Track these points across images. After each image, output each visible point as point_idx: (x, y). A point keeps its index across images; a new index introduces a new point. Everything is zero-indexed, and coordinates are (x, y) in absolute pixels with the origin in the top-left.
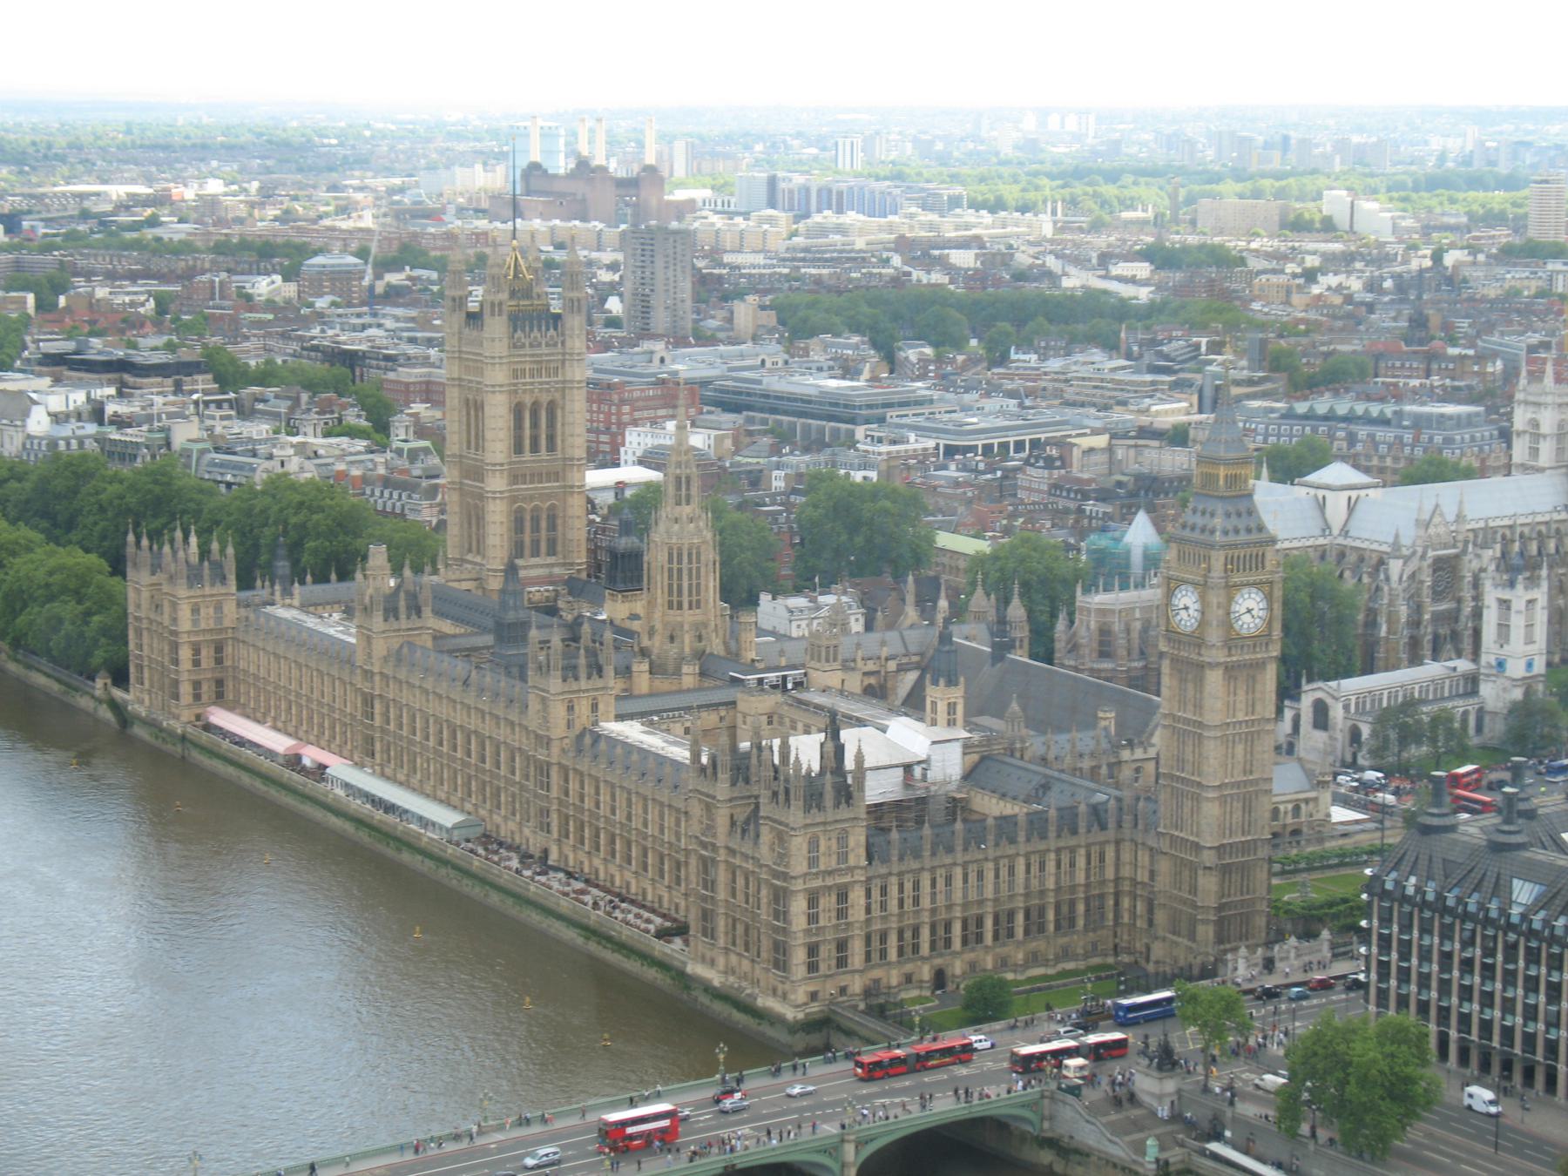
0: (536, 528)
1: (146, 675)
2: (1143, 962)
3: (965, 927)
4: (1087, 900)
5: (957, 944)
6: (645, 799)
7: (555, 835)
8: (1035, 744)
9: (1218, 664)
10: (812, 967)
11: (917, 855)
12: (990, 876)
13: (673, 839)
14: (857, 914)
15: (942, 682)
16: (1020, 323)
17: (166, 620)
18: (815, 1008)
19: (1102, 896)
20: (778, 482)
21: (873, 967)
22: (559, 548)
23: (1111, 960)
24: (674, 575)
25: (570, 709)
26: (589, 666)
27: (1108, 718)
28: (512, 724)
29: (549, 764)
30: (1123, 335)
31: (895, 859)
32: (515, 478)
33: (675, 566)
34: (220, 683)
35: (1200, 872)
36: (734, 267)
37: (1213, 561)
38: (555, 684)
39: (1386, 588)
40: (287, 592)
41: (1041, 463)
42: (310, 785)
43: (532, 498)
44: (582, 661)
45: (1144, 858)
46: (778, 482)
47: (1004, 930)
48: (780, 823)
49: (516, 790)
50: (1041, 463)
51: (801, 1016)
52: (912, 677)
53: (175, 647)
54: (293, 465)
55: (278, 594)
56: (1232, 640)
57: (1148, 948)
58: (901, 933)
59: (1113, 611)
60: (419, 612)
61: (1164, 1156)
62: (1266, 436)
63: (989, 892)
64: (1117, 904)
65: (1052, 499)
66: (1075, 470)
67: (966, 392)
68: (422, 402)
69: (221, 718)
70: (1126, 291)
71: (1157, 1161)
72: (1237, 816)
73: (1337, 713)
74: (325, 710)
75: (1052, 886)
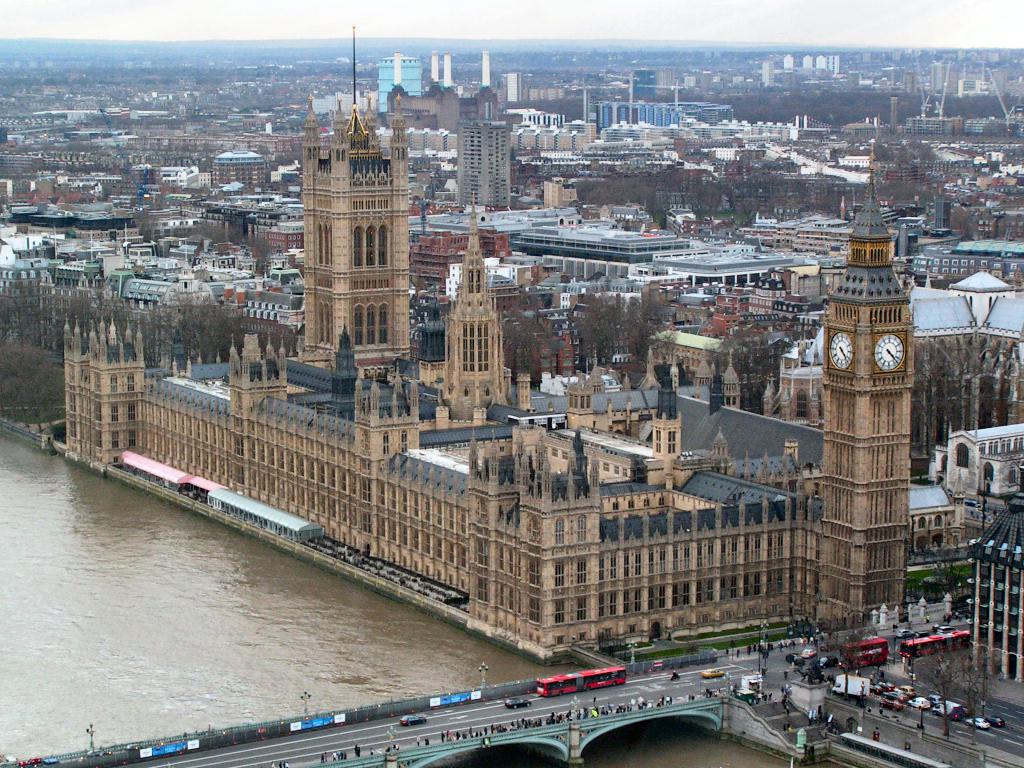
0: (371, 322)
2: (811, 620)
3: (675, 591)
5: (669, 604)
6: (440, 503)
7: (375, 534)
9: (865, 392)
10: (559, 618)
12: (694, 552)
13: (460, 533)
14: (593, 578)
15: (664, 416)
18: (560, 648)
19: (780, 571)
20: (565, 302)
21: (605, 619)
22: (389, 337)
23: (787, 619)
25: (386, 439)
27: (792, 447)
28: (343, 452)
29: (370, 480)
30: (842, 205)
32: (355, 284)
34: (132, 433)
35: (853, 550)
36: (547, 160)
38: (374, 419)
39: (1017, 364)
40: (182, 367)
41: (767, 286)
42: (198, 506)
43: (368, 299)
44: (395, 402)
45: (812, 541)
46: (565, 302)
47: (705, 596)
48: (535, 510)
49: (346, 501)
50: (767, 286)
51: (550, 654)
53: (99, 408)
54: (194, 286)
55: (175, 368)
56: (877, 374)
57: (815, 609)
60: (277, 377)
61: (810, 744)
63: (693, 566)
64: (791, 577)
65: (775, 312)
68: (297, 248)
69: (132, 459)
70: (853, 177)
71: (805, 746)
72: (881, 507)
73: (975, 453)
74: (209, 450)
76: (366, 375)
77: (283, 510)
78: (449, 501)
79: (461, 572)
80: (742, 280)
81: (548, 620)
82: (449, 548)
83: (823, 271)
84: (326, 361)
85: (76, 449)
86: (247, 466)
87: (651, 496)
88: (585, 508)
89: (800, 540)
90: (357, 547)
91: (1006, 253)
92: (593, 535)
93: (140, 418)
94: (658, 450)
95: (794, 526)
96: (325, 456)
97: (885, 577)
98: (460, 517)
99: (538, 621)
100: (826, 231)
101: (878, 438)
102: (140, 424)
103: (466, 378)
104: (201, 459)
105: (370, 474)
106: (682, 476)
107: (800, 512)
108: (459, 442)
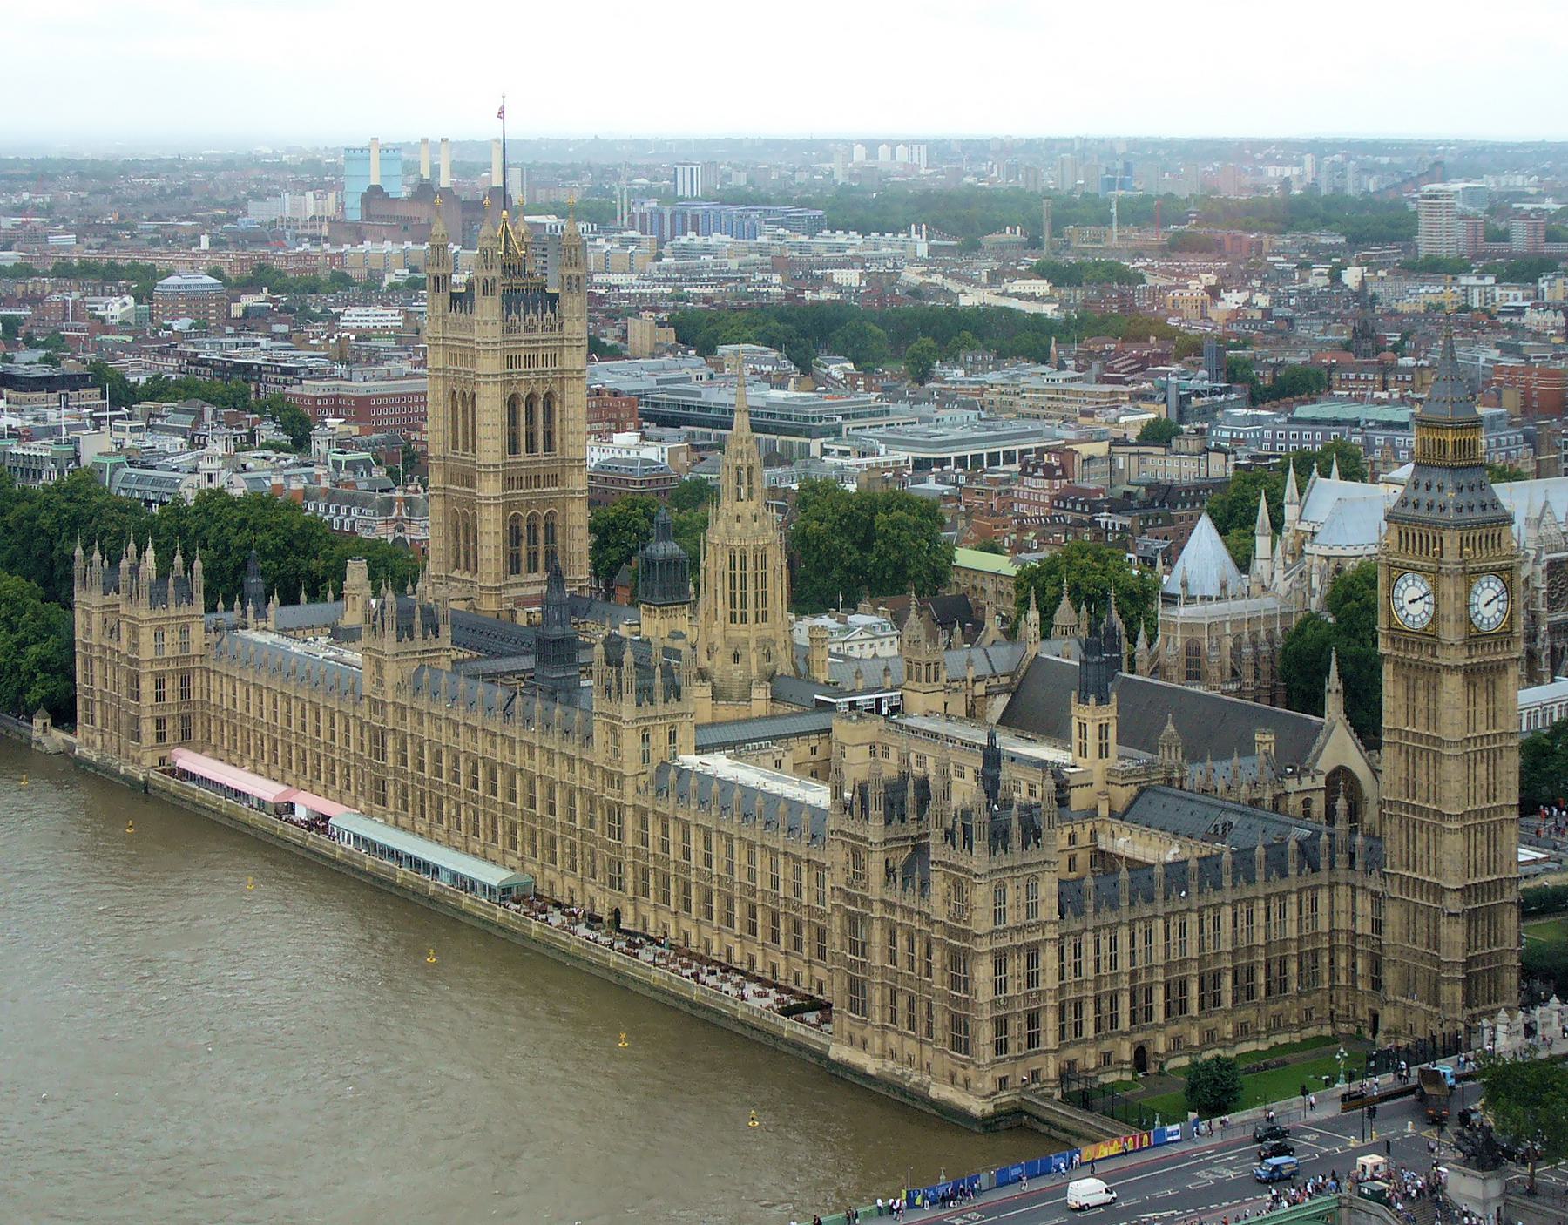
0: (533, 540)
1: (98, 713)
4: (1300, 957)
5: (1159, 1015)
6: (752, 846)
7: (630, 894)
8: (1195, 774)
10: (1000, 1047)
11: (1114, 906)
13: (791, 895)
14: (1049, 981)
17: (124, 647)
19: (1315, 953)
24: (736, 583)
25: (646, 739)
26: (666, 688)
27: (1265, 741)
28: (571, 759)
30: (1053, 348)
31: (1090, 911)
32: (510, 482)
33: (738, 571)
34: (186, 719)
35: (1443, 920)
36: (610, 287)
38: (627, 709)
40: (261, 614)
41: (1040, 473)
43: (529, 504)
44: (658, 681)
45: (1364, 905)
47: (1211, 999)
48: (958, 869)
50: (1040, 473)
52: (1001, 702)
53: (135, 679)
55: (251, 615)
62: (1273, 443)
63: (1193, 951)
64: (1332, 962)
66: (1077, 480)
67: (917, 402)
68: (334, 417)
69: (187, 760)
70: (1031, 308)
72: (1482, 851)
75: (1262, 942)
76: (529, 621)
80: (977, 459)
81: (986, 1053)
83: (1114, 449)
85: (94, 742)
87: (1078, 829)
88: (1037, 864)
89: (1343, 902)
90: (598, 911)
91: (1367, 422)
92: (1048, 909)
93: (198, 697)
94: (1083, 752)
95: (1334, 880)
96: (537, 766)
97: (1490, 963)
98: (790, 870)
99: (966, 1053)
102: (198, 705)
103: (734, 634)
105: (621, 796)
106: (1123, 795)
108: (750, 741)
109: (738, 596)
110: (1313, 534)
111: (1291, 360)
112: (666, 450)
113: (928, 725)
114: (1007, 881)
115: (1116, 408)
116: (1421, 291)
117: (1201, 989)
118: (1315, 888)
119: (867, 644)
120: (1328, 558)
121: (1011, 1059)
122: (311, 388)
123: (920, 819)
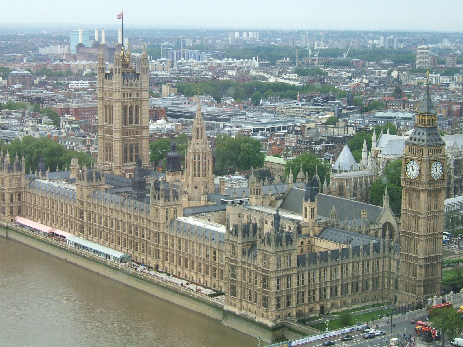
0: (131, 152)
3: (331, 290)
5: (328, 297)
6: (200, 245)
7: (162, 260)
9: (426, 190)
10: (278, 306)
12: (340, 270)
13: (213, 260)
14: (294, 286)
16: (263, 92)
18: (279, 321)
19: (378, 278)
21: (299, 306)
23: (381, 302)
25: (167, 212)
26: (174, 196)
28: (143, 219)
29: (158, 233)
30: (298, 95)
31: (307, 264)
32: (124, 133)
33: (197, 161)
36: (156, 75)
37: (424, 152)
38: (161, 202)
40: (44, 174)
41: (294, 133)
42: (61, 243)
43: (130, 141)
45: (394, 263)
47: (344, 291)
48: (266, 251)
50: (294, 133)
51: (274, 324)
52: (280, 202)
54: (31, 133)
55: (40, 175)
56: (432, 181)
58: (309, 292)
59: (344, 179)
63: (339, 277)
64: (383, 281)
69: (20, 220)
70: (291, 83)
75: (361, 274)
76: (130, 177)
77: (107, 246)
78: (206, 244)
79: (213, 280)
80: (273, 129)
82: (205, 267)
84: (110, 170)
86: (85, 225)
87: (304, 240)
88: (291, 250)
90: (151, 266)
91: (399, 118)
92: (294, 264)
93: (23, 200)
94: (306, 216)
98: (212, 252)
99: (267, 307)
100: (302, 107)
101: (431, 212)
102: (24, 203)
103: (195, 180)
104: (59, 221)
105: (159, 230)
106: (317, 230)
107: (387, 249)
109: (197, 168)
110: (381, 151)
111: (374, 99)
112: (174, 125)
113: (257, 208)
114: (281, 255)
115: (318, 113)
116: (417, 78)
117: (342, 288)
118: (378, 258)
119: (238, 185)
120: (385, 159)
121: (281, 309)
122: (60, 105)
123: (254, 236)
